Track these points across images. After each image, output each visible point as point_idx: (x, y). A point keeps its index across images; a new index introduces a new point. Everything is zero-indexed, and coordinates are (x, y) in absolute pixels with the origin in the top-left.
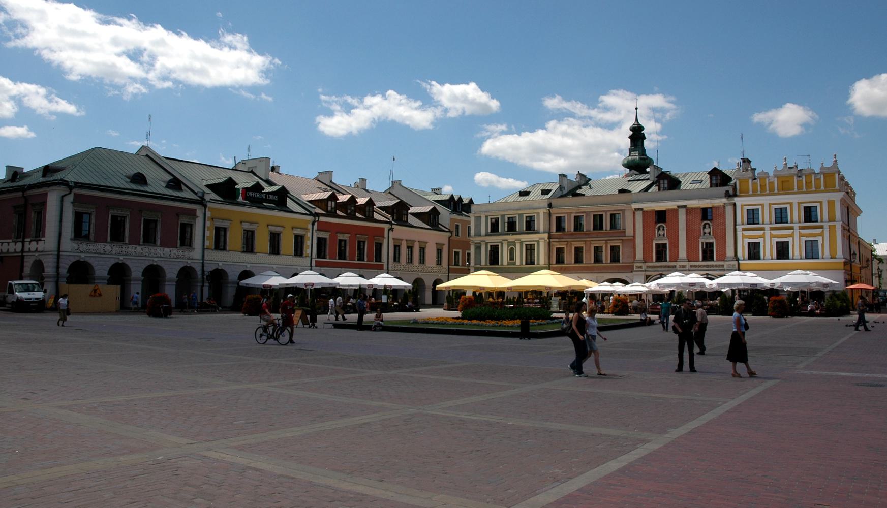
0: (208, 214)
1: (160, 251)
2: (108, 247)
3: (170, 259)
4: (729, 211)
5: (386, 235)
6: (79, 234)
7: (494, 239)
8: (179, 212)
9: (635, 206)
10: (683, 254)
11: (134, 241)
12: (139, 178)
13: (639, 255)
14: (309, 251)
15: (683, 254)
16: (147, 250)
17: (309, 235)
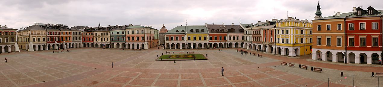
0: (187, 35)
1: (179, 41)
2: (171, 41)
3: (181, 42)
4: (275, 30)
5: (227, 35)
6: (167, 39)
7: (246, 35)
8: (181, 36)
9: (262, 29)
10: (268, 41)
11: (175, 40)
12: (177, 31)
13: (263, 40)
14: (208, 39)
15: (268, 41)
16: (177, 41)
17: (208, 36)
